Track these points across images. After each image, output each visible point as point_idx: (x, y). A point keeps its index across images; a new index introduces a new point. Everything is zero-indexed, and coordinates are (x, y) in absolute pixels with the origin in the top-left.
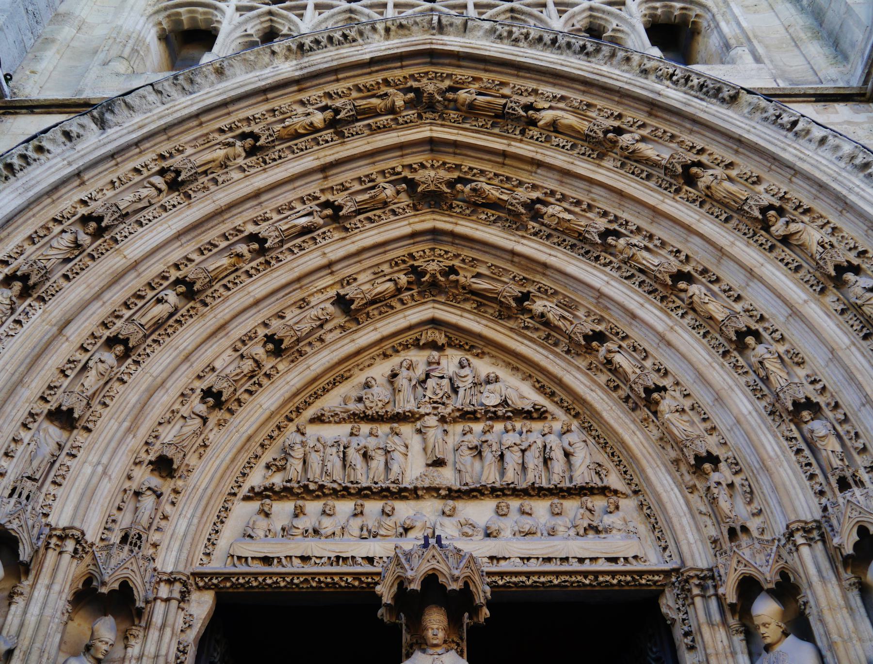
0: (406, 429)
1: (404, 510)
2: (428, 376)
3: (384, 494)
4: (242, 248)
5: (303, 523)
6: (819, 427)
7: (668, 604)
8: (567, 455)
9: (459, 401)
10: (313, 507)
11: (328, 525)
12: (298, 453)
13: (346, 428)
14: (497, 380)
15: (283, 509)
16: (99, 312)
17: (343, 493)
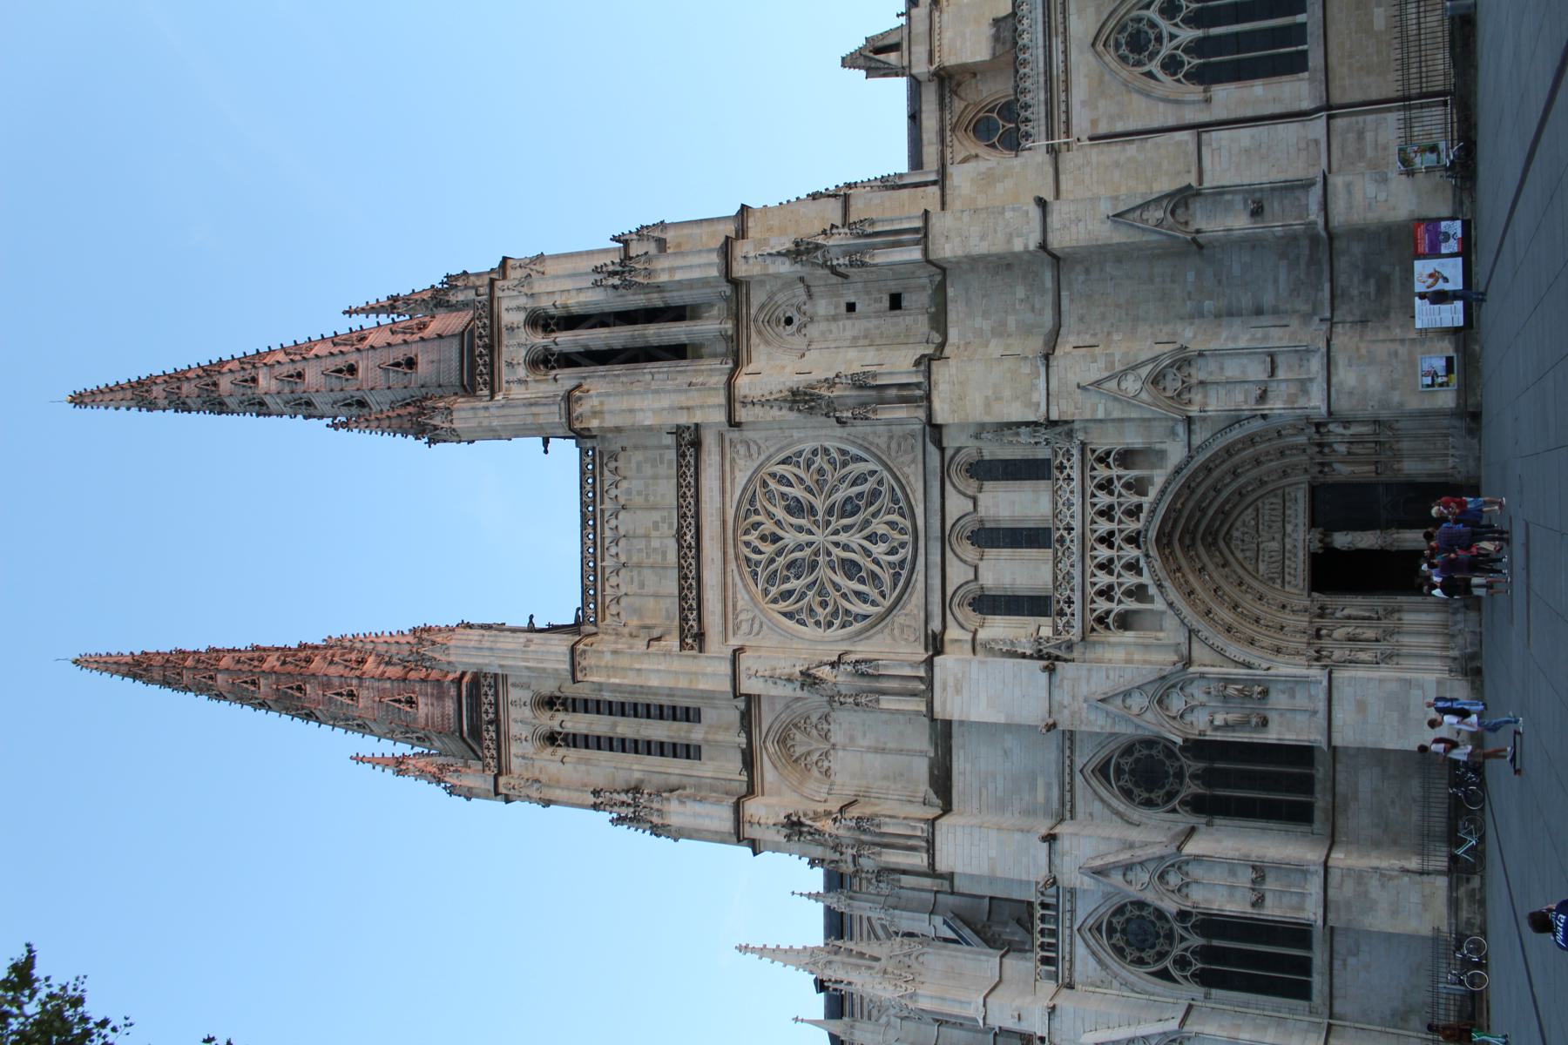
0: (1261, 547)
1: (1288, 547)
2: (1243, 541)
3: (1284, 552)
4: (1220, 593)
5: (1292, 572)
6: (1287, 452)
7: (1315, 484)
8: (1272, 504)
9: (1254, 533)
10: (1287, 570)
11: (1293, 566)
12: (1271, 575)
13: (1260, 563)
14: (1244, 521)
15: (1287, 578)
16: (1249, 625)
17: (1284, 562)
